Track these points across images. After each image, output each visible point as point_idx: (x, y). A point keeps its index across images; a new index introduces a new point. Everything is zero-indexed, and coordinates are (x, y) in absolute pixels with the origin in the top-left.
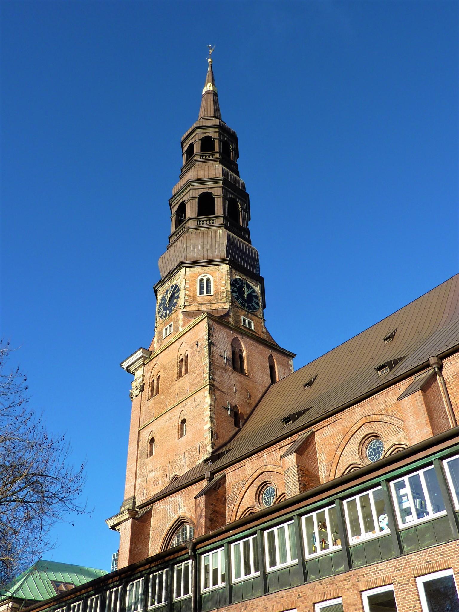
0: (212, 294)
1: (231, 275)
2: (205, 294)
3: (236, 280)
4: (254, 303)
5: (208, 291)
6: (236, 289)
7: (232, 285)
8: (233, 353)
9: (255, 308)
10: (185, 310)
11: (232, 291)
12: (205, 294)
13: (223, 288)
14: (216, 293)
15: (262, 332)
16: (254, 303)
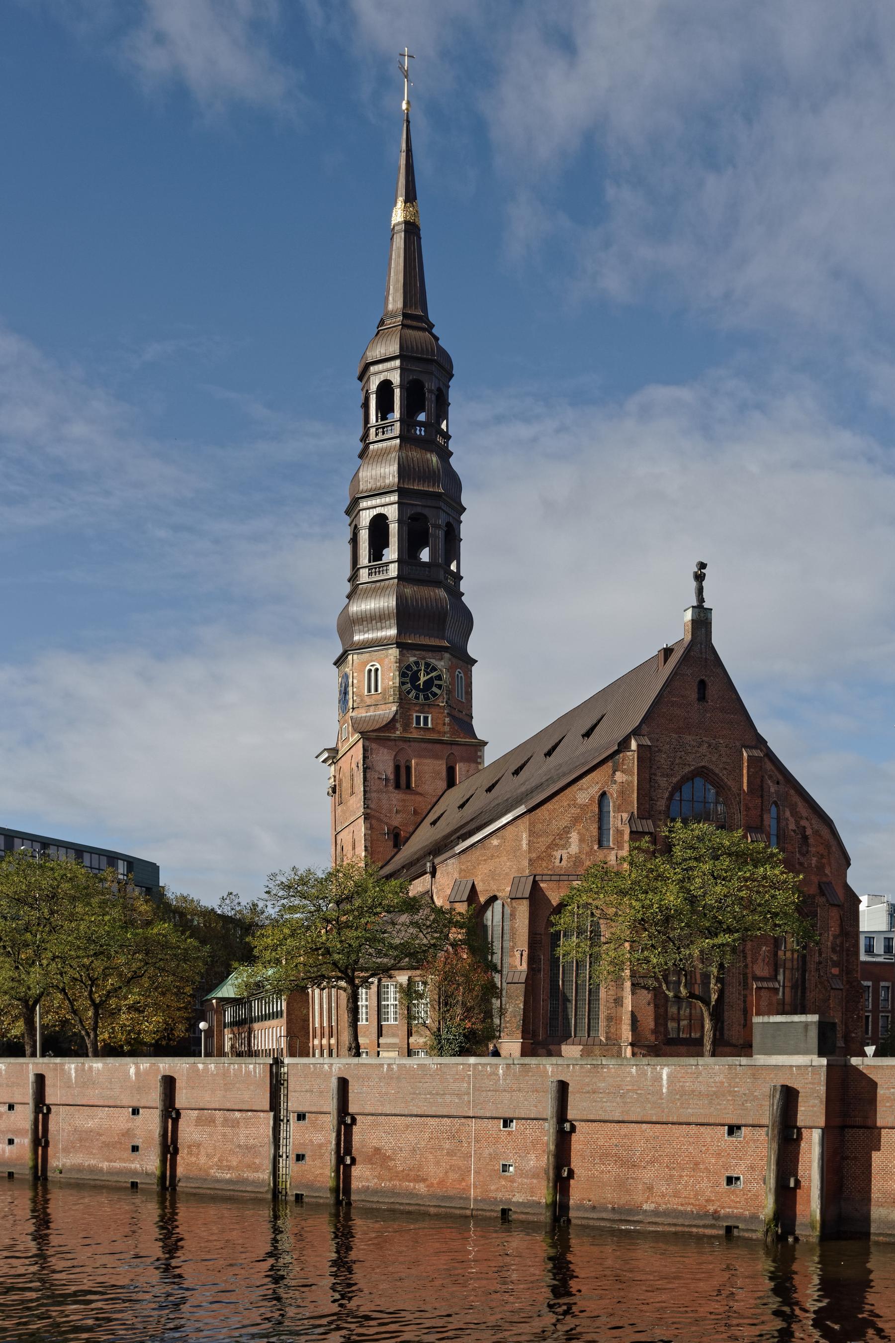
0: (380, 691)
1: (400, 661)
2: (373, 692)
3: (408, 667)
4: (434, 689)
5: (376, 690)
6: (407, 680)
7: (403, 675)
8: (397, 768)
9: (435, 695)
10: (353, 714)
11: (402, 683)
12: (373, 692)
13: (391, 683)
14: (384, 690)
15: (444, 724)
16: (434, 689)
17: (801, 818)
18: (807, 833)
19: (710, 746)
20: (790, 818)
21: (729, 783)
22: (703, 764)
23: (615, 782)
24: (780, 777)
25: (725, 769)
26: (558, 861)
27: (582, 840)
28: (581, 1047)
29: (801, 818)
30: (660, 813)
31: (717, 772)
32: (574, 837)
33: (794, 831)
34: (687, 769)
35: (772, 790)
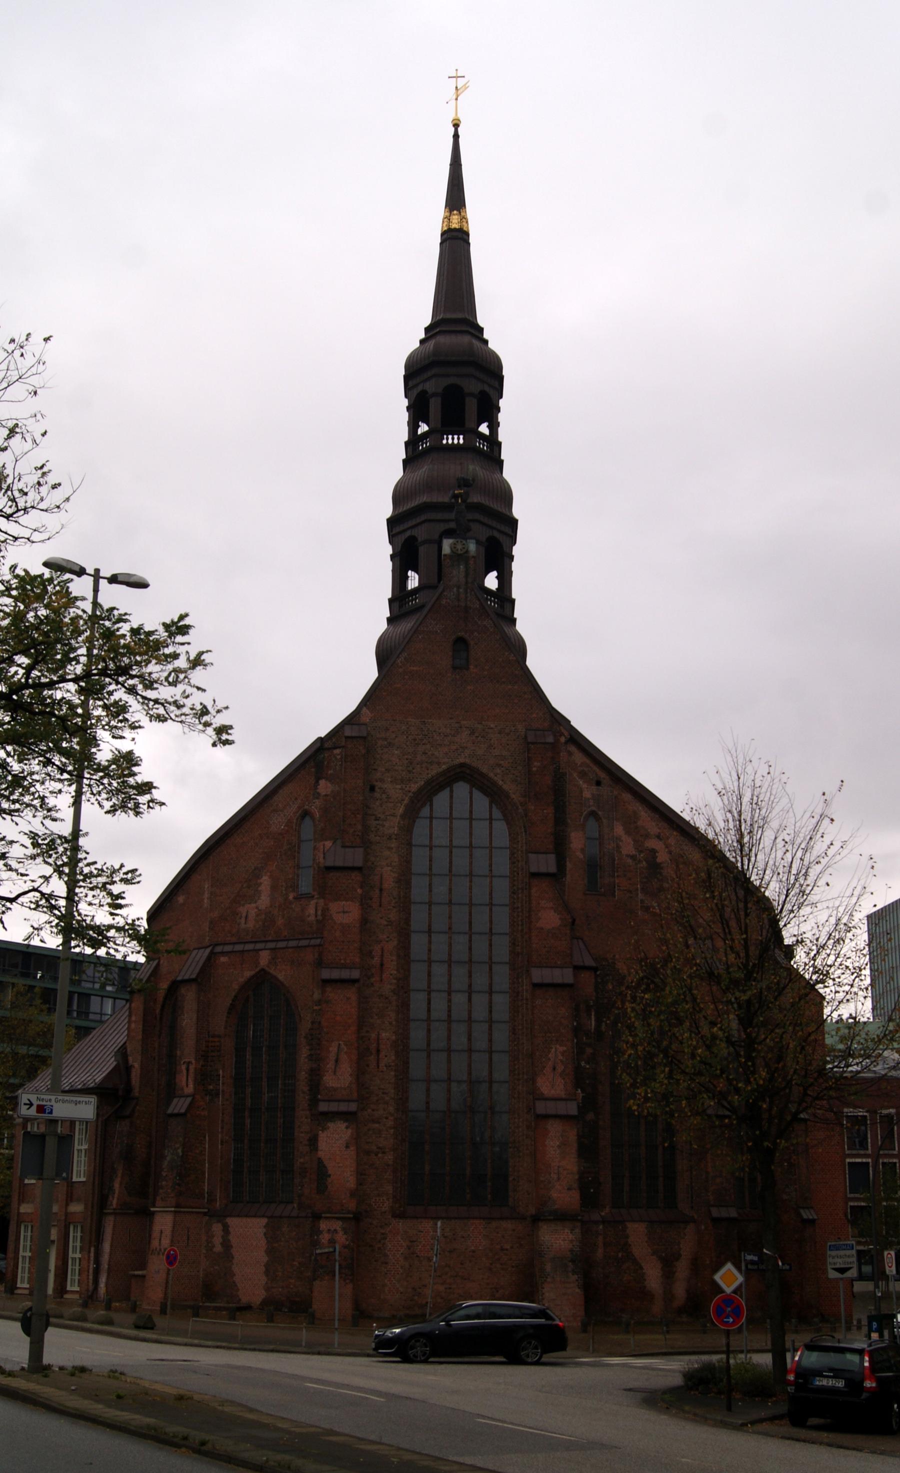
17: (647, 836)
18: (659, 860)
19: (472, 733)
20: (624, 837)
21: (505, 787)
22: (462, 760)
23: (317, 796)
24: (602, 775)
25: (499, 765)
26: (243, 921)
27: (274, 888)
28: (264, 1221)
29: (647, 836)
30: (390, 838)
31: (485, 771)
32: (265, 881)
33: (633, 857)
34: (434, 771)
35: (587, 794)
